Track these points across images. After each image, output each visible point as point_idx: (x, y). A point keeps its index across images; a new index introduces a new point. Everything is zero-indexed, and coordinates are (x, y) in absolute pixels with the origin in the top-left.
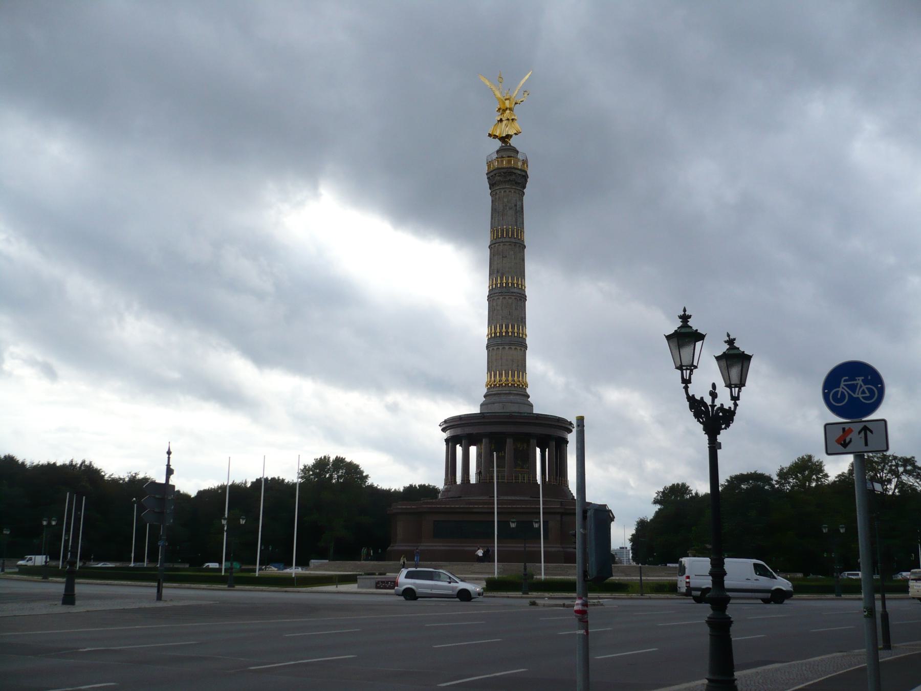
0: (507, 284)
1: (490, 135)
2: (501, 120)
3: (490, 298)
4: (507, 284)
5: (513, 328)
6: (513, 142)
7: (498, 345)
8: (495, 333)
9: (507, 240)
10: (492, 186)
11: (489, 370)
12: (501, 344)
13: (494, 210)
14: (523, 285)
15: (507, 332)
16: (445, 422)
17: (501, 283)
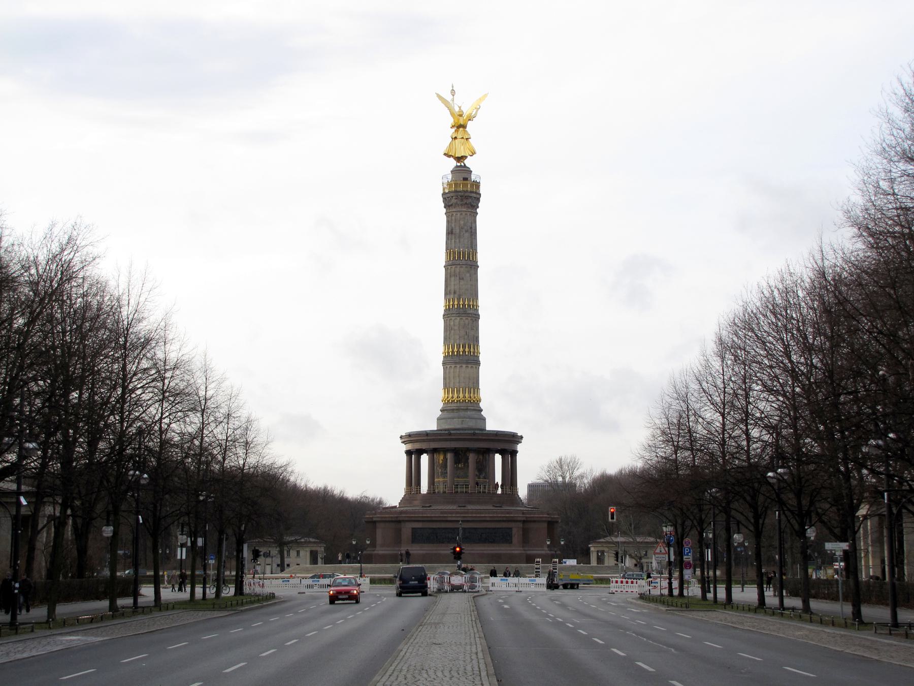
0: (464, 305)
1: (445, 154)
2: (456, 138)
3: (445, 316)
4: (464, 305)
5: (469, 347)
6: (468, 162)
7: (456, 363)
8: (453, 352)
9: (464, 262)
10: (447, 206)
11: (446, 386)
12: (459, 363)
13: (450, 232)
14: (477, 306)
15: (464, 351)
16: (410, 435)
17: (458, 304)
